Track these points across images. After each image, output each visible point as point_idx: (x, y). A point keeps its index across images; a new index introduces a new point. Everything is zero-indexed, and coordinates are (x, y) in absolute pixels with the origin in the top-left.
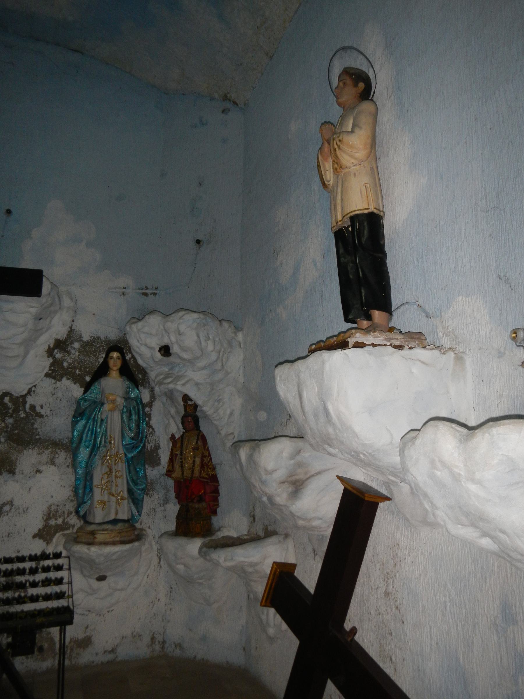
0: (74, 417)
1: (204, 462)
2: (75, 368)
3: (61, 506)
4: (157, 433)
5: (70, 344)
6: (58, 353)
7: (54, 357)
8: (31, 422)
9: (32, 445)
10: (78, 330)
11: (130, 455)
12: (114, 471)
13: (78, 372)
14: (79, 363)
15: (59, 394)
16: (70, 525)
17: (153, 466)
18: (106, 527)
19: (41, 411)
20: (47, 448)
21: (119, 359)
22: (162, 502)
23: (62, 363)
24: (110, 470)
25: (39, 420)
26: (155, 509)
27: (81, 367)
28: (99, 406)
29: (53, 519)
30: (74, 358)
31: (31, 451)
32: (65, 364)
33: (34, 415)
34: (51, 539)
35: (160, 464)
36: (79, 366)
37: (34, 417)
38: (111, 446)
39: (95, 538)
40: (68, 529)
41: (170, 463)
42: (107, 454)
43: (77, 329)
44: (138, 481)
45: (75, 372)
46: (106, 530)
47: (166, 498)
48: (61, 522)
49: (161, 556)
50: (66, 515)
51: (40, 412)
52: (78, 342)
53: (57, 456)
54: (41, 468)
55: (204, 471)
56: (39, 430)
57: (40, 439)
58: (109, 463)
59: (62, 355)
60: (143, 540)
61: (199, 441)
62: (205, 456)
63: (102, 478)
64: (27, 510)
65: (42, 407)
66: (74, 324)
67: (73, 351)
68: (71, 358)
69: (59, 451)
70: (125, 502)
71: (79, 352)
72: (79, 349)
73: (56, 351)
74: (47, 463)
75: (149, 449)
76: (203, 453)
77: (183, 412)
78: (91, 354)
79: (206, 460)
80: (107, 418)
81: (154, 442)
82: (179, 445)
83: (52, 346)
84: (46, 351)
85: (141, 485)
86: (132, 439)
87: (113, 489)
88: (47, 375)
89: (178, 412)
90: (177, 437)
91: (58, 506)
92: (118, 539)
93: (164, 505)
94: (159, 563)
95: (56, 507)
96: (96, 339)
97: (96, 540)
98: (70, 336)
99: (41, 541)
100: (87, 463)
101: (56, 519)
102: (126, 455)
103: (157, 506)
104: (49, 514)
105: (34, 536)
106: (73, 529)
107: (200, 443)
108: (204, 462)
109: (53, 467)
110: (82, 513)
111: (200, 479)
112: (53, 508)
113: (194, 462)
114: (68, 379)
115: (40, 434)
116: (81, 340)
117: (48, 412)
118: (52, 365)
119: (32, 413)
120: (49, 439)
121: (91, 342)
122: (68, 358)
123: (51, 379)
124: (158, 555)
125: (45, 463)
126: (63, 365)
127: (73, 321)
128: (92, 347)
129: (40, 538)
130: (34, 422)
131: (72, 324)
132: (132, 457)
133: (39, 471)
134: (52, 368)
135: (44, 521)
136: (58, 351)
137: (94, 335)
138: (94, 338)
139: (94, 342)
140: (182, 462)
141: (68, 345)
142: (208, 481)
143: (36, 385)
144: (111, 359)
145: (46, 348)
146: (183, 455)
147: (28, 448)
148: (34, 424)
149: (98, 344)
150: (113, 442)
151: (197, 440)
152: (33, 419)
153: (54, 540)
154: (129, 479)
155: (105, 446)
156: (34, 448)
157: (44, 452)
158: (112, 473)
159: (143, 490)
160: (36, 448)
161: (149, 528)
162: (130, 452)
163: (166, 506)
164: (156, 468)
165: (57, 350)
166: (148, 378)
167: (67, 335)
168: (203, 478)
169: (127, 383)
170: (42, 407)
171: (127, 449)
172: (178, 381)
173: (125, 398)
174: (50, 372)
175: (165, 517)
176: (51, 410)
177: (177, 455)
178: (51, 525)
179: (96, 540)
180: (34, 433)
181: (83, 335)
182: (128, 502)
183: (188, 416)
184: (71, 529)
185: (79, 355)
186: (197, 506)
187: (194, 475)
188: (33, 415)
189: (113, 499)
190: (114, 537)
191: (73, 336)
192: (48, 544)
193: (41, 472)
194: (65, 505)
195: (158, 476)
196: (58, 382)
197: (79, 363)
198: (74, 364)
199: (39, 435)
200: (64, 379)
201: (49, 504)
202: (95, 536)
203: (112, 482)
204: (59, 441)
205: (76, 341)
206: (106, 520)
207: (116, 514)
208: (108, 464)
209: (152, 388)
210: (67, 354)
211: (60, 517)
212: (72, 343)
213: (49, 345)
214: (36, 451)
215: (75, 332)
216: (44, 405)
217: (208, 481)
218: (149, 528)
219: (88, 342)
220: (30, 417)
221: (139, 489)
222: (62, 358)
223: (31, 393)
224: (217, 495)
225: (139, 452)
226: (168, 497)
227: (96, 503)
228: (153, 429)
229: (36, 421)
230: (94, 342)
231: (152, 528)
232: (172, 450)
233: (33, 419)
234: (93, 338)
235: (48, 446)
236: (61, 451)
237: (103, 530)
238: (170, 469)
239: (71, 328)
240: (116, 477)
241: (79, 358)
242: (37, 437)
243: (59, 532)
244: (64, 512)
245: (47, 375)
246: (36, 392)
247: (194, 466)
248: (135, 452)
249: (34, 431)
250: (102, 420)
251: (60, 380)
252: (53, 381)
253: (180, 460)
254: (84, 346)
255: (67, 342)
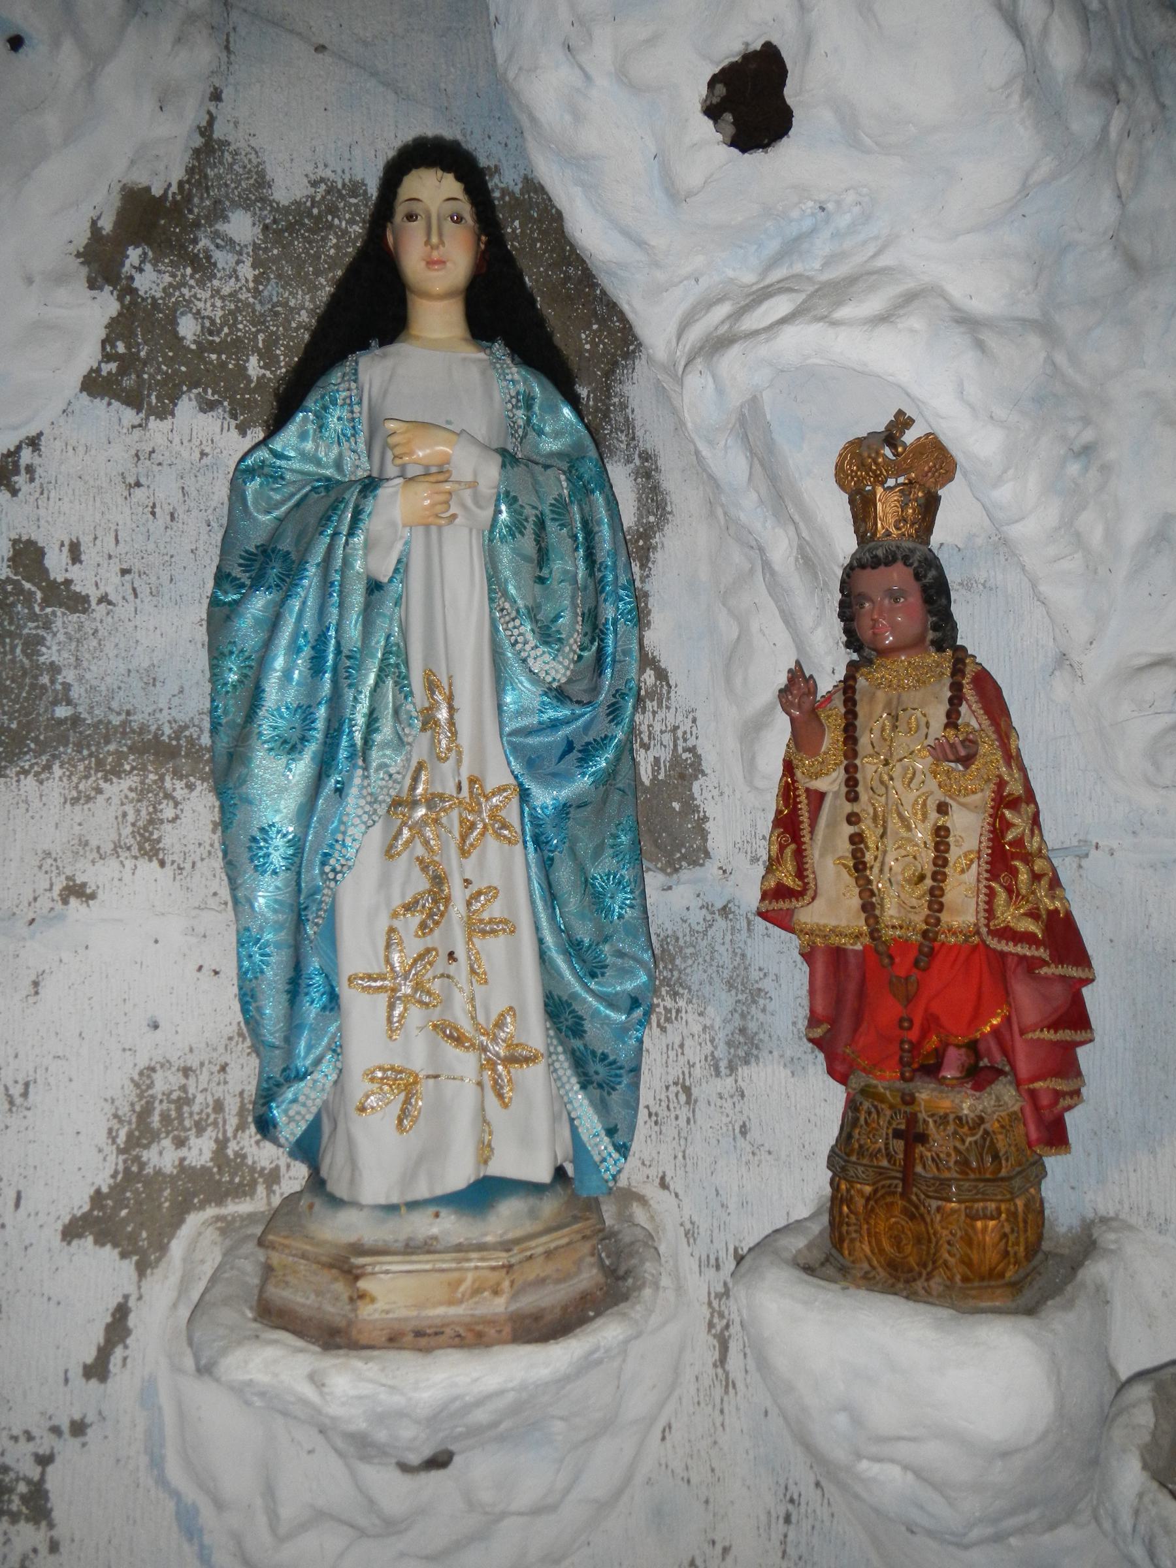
0: (222, 578)
1: (1010, 836)
2: (237, 347)
3: (204, 1077)
4: (683, 692)
5: (207, 217)
6: (148, 267)
7: (127, 291)
8: (26, 631)
9: (38, 754)
10: (242, 144)
11: (545, 798)
12: (458, 893)
13: (254, 367)
14: (258, 321)
15: (165, 488)
16: (252, 1169)
17: (672, 868)
18: (424, 1225)
19: (75, 572)
20: (116, 772)
21: (459, 220)
22: (721, 1052)
23: (174, 323)
24: (439, 880)
25: (65, 620)
26: (687, 1090)
27: (271, 342)
28: (352, 496)
29: (167, 1143)
30: (233, 295)
31: (29, 782)
32: (188, 328)
33: (39, 595)
34: (163, 1249)
35: (707, 855)
36: (261, 337)
37: (37, 609)
38: (434, 744)
39: (362, 1296)
40: (245, 1190)
41: (782, 848)
42: (413, 788)
43: (238, 139)
44: (606, 948)
45: (242, 370)
46: (427, 1247)
47: (743, 1031)
48: (207, 1155)
49: (727, 1326)
50: (233, 1121)
51: (68, 582)
52: (247, 208)
53: (168, 812)
54: (88, 874)
55: (1009, 890)
56: (69, 675)
57: (76, 720)
58: (426, 843)
59: (167, 279)
60: (647, 1292)
61: (964, 709)
62: (1013, 803)
63: (392, 930)
64: (25, 1095)
65: (75, 552)
66: (224, 112)
67: (223, 259)
68: (216, 292)
69: (179, 784)
70: (534, 1077)
71: (254, 266)
72: (256, 247)
73: (134, 255)
74: (117, 847)
75: (646, 776)
76: (1001, 784)
77: (846, 544)
78: (317, 273)
79: (1018, 822)
80: (402, 567)
81: (667, 738)
82: (832, 739)
83: (107, 225)
84: (78, 255)
85: (625, 973)
86: (560, 695)
87: (459, 1000)
88: (93, 385)
89: (807, 560)
90: (826, 684)
91: (186, 1071)
92: (499, 1305)
93: (732, 1068)
94: (722, 1360)
95: (177, 1080)
96: (342, 197)
97: (367, 1312)
98: (206, 176)
99: (109, 1253)
100: (297, 845)
101: (180, 1143)
102: (524, 795)
103: (697, 1072)
104: (144, 1115)
105: (72, 1232)
106: (270, 1191)
107: (971, 716)
108: (1010, 836)
109: (148, 868)
110: (291, 1129)
111: (993, 943)
112: (163, 1083)
113: (941, 835)
114: (207, 406)
115: (74, 694)
116: (263, 200)
117: (112, 584)
118: (118, 328)
119: (27, 585)
120: (124, 724)
121: (315, 211)
122: (202, 294)
123: (116, 404)
124: (711, 1325)
125: (108, 847)
126: (175, 333)
127: (216, 96)
128: (325, 239)
129: (100, 1242)
130: (41, 632)
131: (209, 113)
132: (564, 810)
133: (76, 891)
134: (121, 348)
135: (120, 1151)
136: (145, 254)
137: (327, 174)
138: (328, 192)
139: (333, 210)
140: (857, 840)
141: (196, 225)
142: (1042, 953)
143: (41, 434)
144: (411, 217)
145: (82, 238)
146: (864, 797)
147: (12, 772)
148: (41, 641)
149: (351, 222)
150: (443, 715)
151: (956, 700)
152: (34, 617)
153: (177, 1247)
154: (549, 939)
155: (400, 742)
156: (48, 767)
157: (99, 791)
158: (448, 900)
159: (635, 1002)
160: (57, 771)
161: (663, 1185)
162: (553, 778)
163: (743, 1071)
164: (686, 874)
165: (139, 251)
166: (623, 406)
167: (190, 171)
168: (1008, 934)
169: (515, 372)
170: (75, 552)
171: (532, 762)
172: (839, 304)
173: (503, 452)
174: (113, 367)
175: (744, 1130)
176: (125, 572)
177: (818, 798)
178: (158, 1172)
179: (367, 1312)
180: (43, 687)
181: (274, 172)
182: (552, 1069)
183: (889, 560)
184: (261, 1190)
185: (257, 280)
186: (967, 1104)
187: (944, 917)
188: (31, 594)
189: (464, 1062)
190: (476, 1291)
191: (219, 177)
192: (142, 1269)
193: (92, 896)
194: (223, 1069)
195: (697, 917)
196: (153, 423)
197: (258, 321)
198: (233, 327)
199: (69, 702)
200: (186, 406)
201: (143, 1063)
202: (362, 1284)
203: (451, 955)
204: (177, 735)
205: (235, 205)
206: (422, 1191)
207: (485, 1151)
208: (420, 850)
209: (646, 457)
210: (195, 271)
211: (200, 1129)
212: (218, 213)
213: (94, 223)
214: (57, 784)
215: (228, 158)
216: (86, 541)
217: (1042, 953)
218: (663, 1185)
219: (299, 210)
220: (13, 605)
221: (610, 1002)
222: (170, 295)
223: (15, 478)
224: (1079, 1036)
225: (607, 779)
226: (752, 1026)
227: (358, 1087)
228: (662, 675)
229: (47, 625)
230: (333, 210)
231: (676, 1184)
232: (789, 767)
233: (34, 617)
234: (323, 187)
235: (120, 756)
236: (190, 787)
237: (410, 1249)
238: (789, 882)
239: (206, 131)
240: (476, 928)
241: (256, 293)
242: (62, 712)
243: (202, 1207)
244: (219, 1106)
245: (93, 385)
246: (39, 471)
247: (941, 861)
248: (583, 783)
249: (45, 679)
250: (374, 587)
251: (163, 413)
252: (129, 415)
253: (850, 830)
254: (279, 232)
255: (191, 211)
